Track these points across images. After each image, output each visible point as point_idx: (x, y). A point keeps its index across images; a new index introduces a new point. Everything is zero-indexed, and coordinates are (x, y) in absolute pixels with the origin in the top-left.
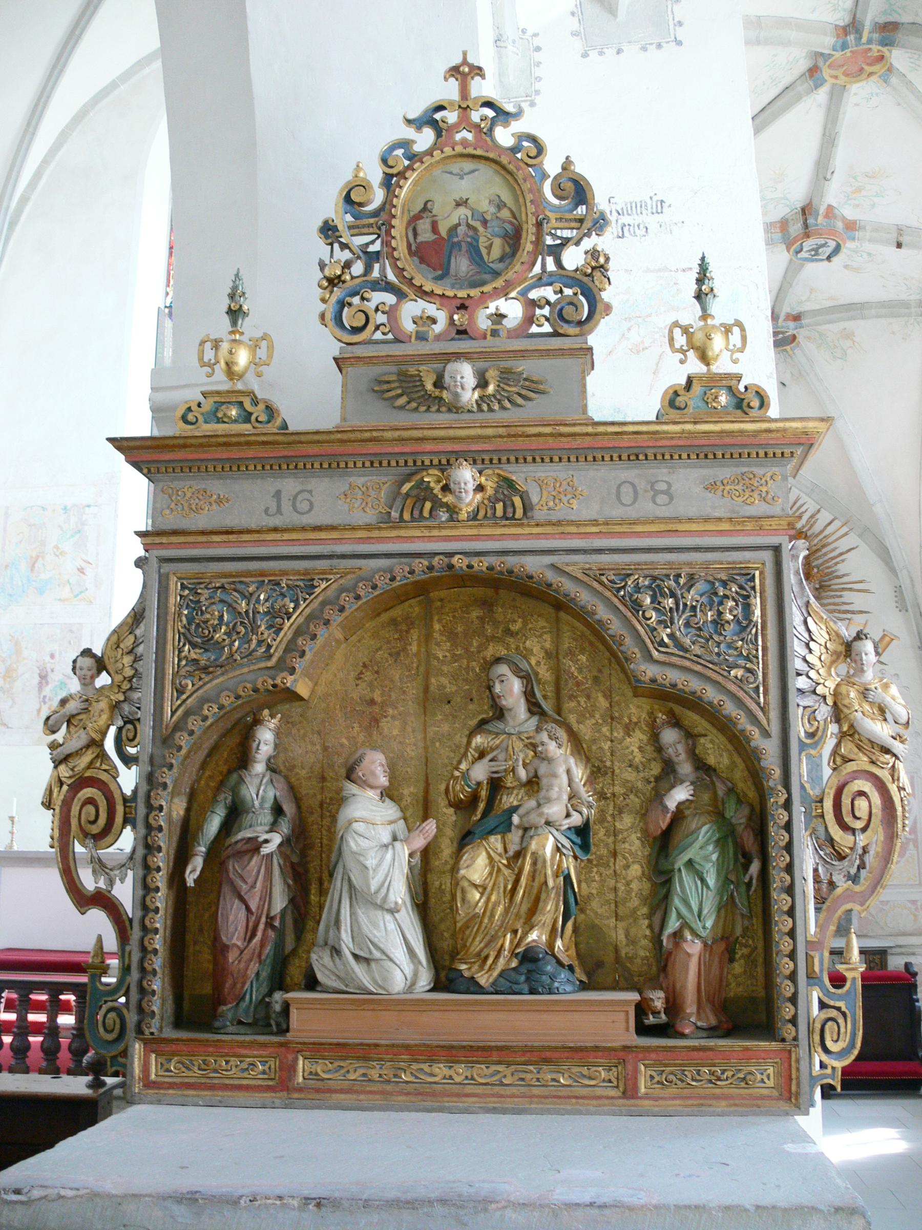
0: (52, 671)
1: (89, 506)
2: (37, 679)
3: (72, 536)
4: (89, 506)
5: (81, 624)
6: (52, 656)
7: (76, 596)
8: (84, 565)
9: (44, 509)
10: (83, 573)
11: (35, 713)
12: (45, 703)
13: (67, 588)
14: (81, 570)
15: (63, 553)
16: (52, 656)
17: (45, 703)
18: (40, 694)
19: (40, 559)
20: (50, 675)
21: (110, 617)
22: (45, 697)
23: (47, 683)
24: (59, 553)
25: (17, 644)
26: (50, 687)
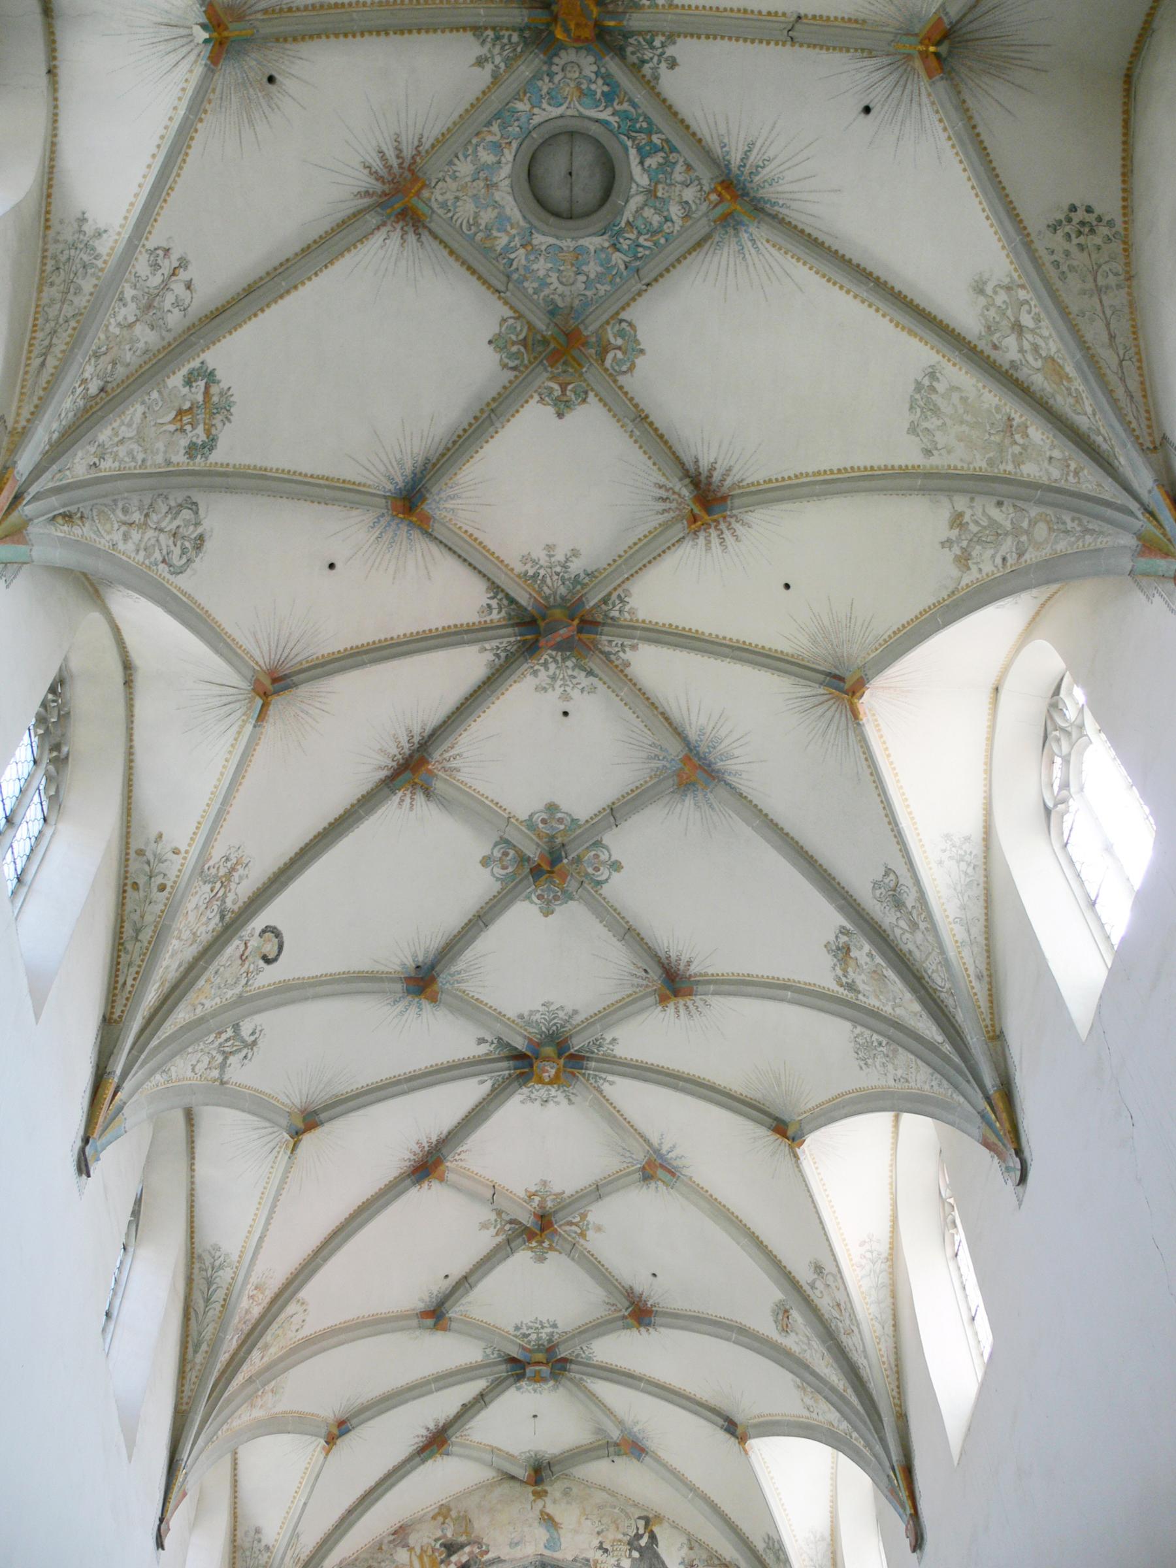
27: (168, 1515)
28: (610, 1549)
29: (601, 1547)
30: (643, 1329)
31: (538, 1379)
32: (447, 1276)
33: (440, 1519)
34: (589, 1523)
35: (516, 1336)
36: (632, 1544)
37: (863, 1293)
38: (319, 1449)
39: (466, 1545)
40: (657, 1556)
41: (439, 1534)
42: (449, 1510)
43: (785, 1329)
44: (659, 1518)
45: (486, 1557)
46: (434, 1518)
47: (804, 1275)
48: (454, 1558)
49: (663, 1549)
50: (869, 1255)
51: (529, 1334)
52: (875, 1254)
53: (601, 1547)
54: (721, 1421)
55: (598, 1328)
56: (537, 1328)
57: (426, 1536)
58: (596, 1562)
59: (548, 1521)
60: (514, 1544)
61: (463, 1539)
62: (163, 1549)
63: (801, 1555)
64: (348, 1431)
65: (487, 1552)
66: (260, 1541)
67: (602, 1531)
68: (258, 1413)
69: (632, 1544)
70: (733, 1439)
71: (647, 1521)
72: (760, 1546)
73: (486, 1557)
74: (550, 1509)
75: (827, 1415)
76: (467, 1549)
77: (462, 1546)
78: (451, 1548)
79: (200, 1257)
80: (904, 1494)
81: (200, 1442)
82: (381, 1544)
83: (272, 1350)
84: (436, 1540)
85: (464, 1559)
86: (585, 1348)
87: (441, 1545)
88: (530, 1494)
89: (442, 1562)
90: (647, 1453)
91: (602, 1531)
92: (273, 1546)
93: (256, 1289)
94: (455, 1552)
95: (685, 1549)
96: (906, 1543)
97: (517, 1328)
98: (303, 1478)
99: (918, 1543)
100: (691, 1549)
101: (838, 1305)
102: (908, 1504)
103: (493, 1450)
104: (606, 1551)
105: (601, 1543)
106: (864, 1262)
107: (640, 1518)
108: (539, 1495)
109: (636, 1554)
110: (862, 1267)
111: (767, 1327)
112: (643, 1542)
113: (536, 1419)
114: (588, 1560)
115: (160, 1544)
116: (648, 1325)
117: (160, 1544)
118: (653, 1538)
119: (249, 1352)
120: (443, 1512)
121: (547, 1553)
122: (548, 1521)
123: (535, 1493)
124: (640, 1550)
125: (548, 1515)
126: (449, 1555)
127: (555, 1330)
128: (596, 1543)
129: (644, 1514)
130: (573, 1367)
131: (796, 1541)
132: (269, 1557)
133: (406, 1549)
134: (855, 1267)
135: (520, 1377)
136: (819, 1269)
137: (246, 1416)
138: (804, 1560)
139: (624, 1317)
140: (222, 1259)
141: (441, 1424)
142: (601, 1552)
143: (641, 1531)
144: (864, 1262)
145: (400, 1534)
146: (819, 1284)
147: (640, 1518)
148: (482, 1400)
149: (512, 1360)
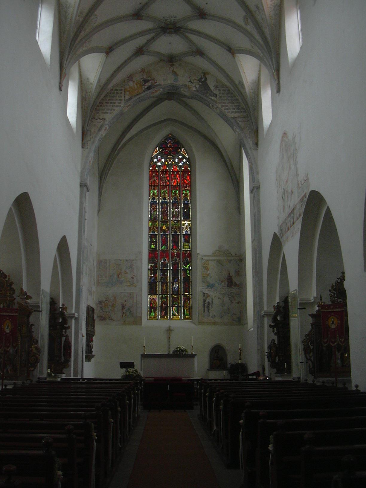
0: (126, 305)
1: (134, 260)
2: (121, 308)
3: (129, 268)
4: (134, 260)
5: (133, 293)
6: (125, 301)
7: (132, 285)
8: (134, 276)
9: (121, 260)
10: (133, 279)
11: (121, 317)
12: (124, 314)
13: (129, 283)
14: (132, 278)
15: (127, 273)
16: (125, 301)
17: (124, 314)
18: (122, 311)
19: (120, 274)
20: (125, 307)
21: (142, 292)
22: (124, 312)
23: (124, 309)
24: (126, 273)
25: (115, 298)
26: (125, 310)
27: (62, 81)
28: (192, 81)
29: (190, 81)
30: (203, 20)
31: (170, 33)
32: (141, 3)
33: (142, 73)
34: (187, 74)
35: (163, 20)
36: (200, 80)
37: (270, 16)
38: (104, 56)
39: (150, 80)
40: (207, 84)
41: (142, 77)
42: (145, 70)
43: (246, 24)
44: (208, 73)
45: (156, 84)
46: (140, 72)
47: (253, 8)
48: (146, 84)
49: (208, 82)
50: (273, 4)
51: (167, 20)
52: (275, 4)
53: (190, 81)
54: (227, 48)
55: (189, 18)
56: (170, 18)
57: (138, 78)
58: (189, 85)
59: (175, 73)
60: (164, 80)
61: (149, 79)
62: (62, 91)
63: (249, 86)
64: (112, 50)
65: (156, 82)
66: (89, 82)
67: (191, 77)
68: (84, 49)
69: (200, 80)
70: (230, 53)
71: (204, 74)
72: (237, 83)
73: (156, 84)
74: (175, 70)
75: (257, 50)
76: (150, 82)
77: (149, 81)
78: (146, 81)
79: (62, 4)
80: (276, 77)
81: (68, 60)
82: (125, 80)
83: (87, 30)
84: (141, 79)
85: (150, 84)
86: (185, 24)
87: (143, 80)
88: (169, 65)
89: (143, 85)
90: (205, 55)
91: (191, 77)
92: (93, 83)
93: (80, 13)
94: (147, 83)
95: (215, 82)
96: (275, 91)
97: (164, 18)
98: (100, 64)
99: (279, 91)
100: (217, 82)
101: (263, 19)
102: (277, 81)
103: (158, 53)
104: (192, 82)
105: (190, 80)
106: (271, 7)
107: (202, 73)
108: (172, 66)
109: (200, 84)
110: (271, 8)
111: (241, 22)
112: (203, 80)
113: (170, 44)
114: (186, 85)
115: (61, 90)
116: (205, 19)
117: (61, 90)
118: (206, 79)
119: (80, 32)
120: (143, 71)
121: (174, 83)
122: (175, 73)
123: (171, 65)
124: (202, 82)
125: (174, 71)
126: (145, 84)
127: (176, 18)
128: (189, 80)
129: (204, 72)
130: (182, 30)
131: (248, 83)
132: (92, 86)
133: (132, 82)
134: (268, 8)
135: (165, 32)
136: (257, 7)
137: (81, 50)
138: (249, 88)
139: (197, 16)
140: (69, 5)
141: (141, 46)
142: (190, 83)
143: (202, 77)
144: (271, 7)
145: (130, 77)
146: (257, 12)
147: (202, 73)
148: (153, 39)
149: (162, 27)
